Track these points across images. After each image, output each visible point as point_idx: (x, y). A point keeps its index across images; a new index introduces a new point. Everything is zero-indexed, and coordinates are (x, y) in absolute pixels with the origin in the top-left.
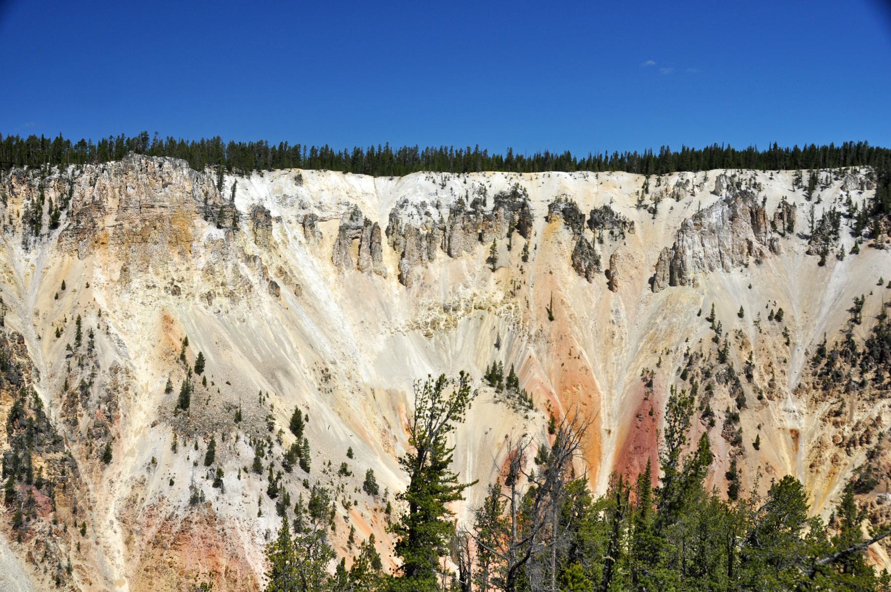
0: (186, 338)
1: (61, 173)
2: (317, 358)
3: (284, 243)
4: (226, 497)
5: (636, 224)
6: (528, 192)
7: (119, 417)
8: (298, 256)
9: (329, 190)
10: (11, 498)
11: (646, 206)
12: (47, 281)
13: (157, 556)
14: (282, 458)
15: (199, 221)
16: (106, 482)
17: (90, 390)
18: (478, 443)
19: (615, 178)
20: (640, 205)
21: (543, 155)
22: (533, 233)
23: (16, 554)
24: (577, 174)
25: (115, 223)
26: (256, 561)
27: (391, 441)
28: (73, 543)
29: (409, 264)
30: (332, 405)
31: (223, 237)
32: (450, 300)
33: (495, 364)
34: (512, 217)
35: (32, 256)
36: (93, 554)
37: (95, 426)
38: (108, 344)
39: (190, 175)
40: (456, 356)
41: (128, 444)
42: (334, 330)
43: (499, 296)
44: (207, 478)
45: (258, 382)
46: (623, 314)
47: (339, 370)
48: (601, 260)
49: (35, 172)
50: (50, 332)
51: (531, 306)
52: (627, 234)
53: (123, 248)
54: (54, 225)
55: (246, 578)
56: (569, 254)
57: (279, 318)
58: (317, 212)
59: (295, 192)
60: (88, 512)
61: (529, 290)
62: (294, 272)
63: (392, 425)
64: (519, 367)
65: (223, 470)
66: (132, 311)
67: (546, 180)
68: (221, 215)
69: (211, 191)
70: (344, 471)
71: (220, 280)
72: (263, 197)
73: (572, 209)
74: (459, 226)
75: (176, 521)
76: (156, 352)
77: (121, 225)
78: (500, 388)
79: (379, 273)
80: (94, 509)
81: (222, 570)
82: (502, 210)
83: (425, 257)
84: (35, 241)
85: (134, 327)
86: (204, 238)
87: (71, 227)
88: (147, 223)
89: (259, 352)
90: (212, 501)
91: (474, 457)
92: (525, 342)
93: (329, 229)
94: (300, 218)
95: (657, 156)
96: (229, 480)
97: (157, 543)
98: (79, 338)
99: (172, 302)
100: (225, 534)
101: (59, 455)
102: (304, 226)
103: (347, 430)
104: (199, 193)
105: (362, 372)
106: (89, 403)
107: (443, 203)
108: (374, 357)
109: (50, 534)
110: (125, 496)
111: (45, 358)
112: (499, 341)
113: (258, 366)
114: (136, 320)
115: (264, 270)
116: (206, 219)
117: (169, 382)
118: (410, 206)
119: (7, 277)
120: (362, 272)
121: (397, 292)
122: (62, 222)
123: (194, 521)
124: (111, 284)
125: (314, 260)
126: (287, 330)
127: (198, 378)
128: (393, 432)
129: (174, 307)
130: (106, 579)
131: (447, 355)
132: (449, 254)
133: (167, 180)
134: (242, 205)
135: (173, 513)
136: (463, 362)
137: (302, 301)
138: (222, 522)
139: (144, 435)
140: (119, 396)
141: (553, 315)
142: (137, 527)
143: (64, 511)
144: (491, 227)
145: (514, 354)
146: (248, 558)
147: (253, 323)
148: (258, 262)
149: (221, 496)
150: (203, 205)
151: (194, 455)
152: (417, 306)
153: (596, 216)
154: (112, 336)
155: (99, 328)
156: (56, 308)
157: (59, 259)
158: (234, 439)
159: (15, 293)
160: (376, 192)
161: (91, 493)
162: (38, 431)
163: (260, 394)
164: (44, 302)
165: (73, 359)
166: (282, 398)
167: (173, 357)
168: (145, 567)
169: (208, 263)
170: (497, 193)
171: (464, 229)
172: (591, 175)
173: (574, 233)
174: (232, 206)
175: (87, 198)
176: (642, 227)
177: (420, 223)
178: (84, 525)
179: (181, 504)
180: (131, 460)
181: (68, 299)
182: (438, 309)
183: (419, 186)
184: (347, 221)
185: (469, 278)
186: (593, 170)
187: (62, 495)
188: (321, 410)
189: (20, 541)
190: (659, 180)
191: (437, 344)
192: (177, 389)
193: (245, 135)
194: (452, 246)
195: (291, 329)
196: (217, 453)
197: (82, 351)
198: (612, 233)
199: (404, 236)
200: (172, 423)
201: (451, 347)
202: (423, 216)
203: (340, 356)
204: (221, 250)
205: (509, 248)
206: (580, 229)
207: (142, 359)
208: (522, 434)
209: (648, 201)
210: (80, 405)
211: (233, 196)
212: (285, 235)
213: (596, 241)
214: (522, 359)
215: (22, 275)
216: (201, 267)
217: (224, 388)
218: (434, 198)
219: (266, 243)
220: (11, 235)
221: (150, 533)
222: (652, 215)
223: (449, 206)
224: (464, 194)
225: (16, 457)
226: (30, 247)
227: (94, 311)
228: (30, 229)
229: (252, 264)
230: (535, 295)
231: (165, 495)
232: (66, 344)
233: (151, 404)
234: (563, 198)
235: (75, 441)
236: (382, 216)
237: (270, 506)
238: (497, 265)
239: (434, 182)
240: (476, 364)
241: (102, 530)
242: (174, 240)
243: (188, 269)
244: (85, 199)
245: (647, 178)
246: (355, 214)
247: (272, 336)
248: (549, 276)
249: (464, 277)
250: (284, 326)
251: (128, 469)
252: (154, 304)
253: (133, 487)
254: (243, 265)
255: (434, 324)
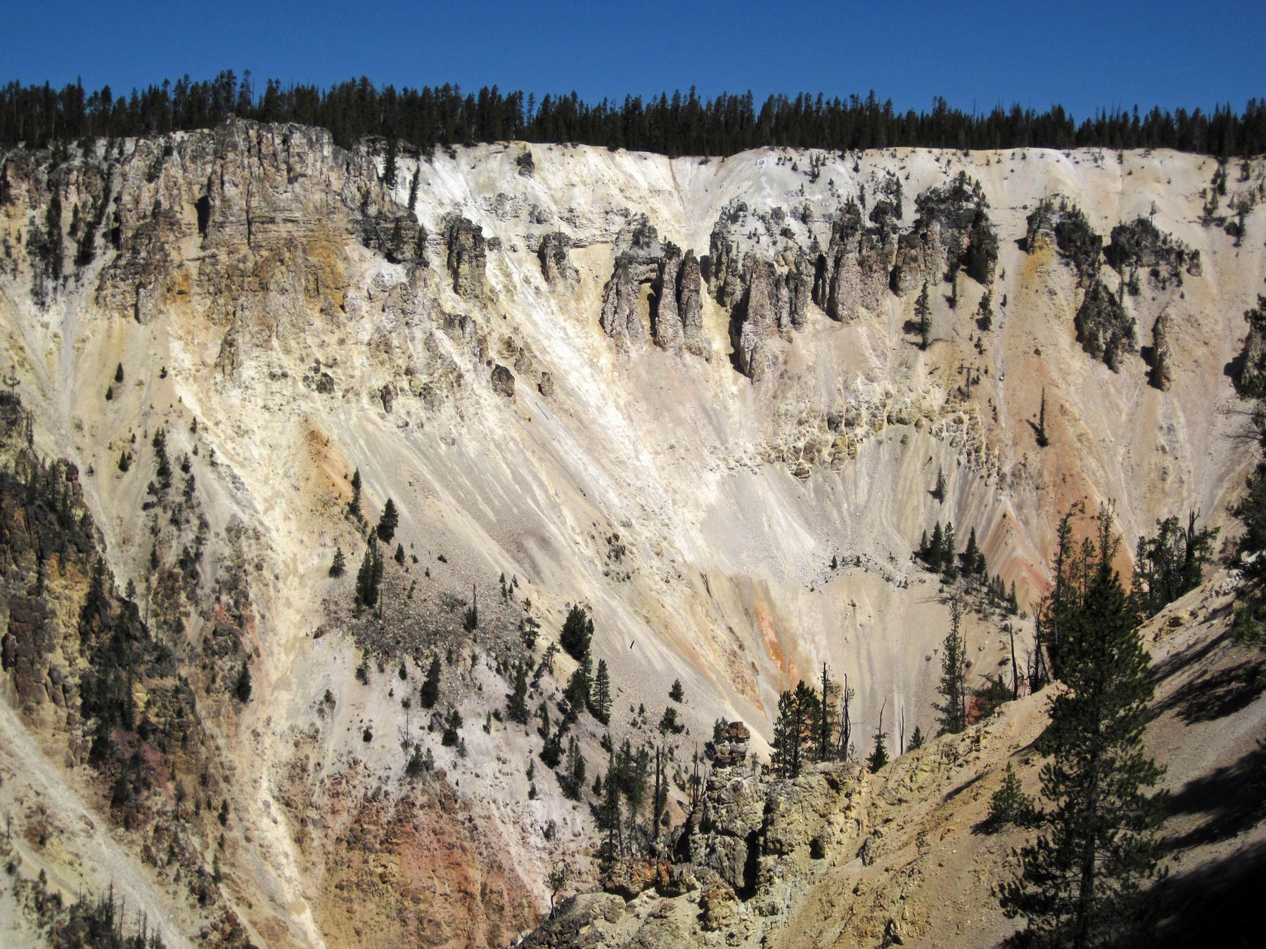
0: (357, 475)
1: (85, 155)
2: (596, 516)
3: (509, 291)
4: (469, 762)
5: (1203, 258)
6: (986, 189)
7: (253, 618)
8: (536, 317)
9: (584, 183)
10: (99, 754)
11: (1220, 221)
12: (85, 366)
13: (357, 862)
14: (560, 696)
15: (354, 248)
16: (246, 736)
17: (198, 568)
18: (913, 677)
19: (1156, 162)
20: (1209, 218)
21: (1008, 114)
22: (998, 272)
23: (125, 849)
24: (1079, 153)
25: (202, 254)
26: (533, 876)
27: (748, 673)
28: (211, 835)
29: (755, 333)
30: (632, 604)
31: (405, 280)
32: (839, 405)
33: (937, 528)
34: (956, 241)
35: (52, 318)
36: (247, 857)
37: (215, 633)
38: (216, 485)
39: (335, 158)
40: (858, 515)
41: (276, 668)
42: (621, 462)
43: (937, 398)
44: (431, 728)
45: (495, 559)
46: (1182, 434)
47: (639, 536)
48: (1137, 328)
49: (39, 154)
50: (107, 464)
51: (1002, 418)
52: (1185, 277)
53: (221, 301)
54: (85, 257)
55: (521, 905)
56: (1070, 315)
57: (518, 439)
58: (566, 229)
59: (520, 188)
60: (223, 785)
61: (995, 387)
62: (534, 348)
63: (746, 644)
64: (983, 537)
65: (462, 713)
66: (248, 423)
67: (1017, 164)
68: (397, 236)
69: (374, 188)
70: (669, 723)
71: (402, 363)
72: (459, 198)
73: (1074, 224)
74: (852, 258)
75: (385, 803)
76: (303, 501)
77: (214, 256)
78: (949, 577)
79: (697, 352)
80: (233, 781)
81: (476, 889)
82: (936, 227)
83: (785, 319)
84: (55, 289)
85: (256, 453)
86: (368, 282)
87: (123, 262)
88: (265, 253)
89: (489, 502)
90: (446, 769)
91: (908, 703)
92: (993, 488)
93: (592, 262)
94: (533, 242)
95: (1239, 117)
96: (470, 732)
97: (354, 840)
98: (164, 471)
99: (319, 405)
100: (476, 828)
101: (170, 682)
102: (542, 256)
103: (664, 649)
104: (352, 192)
105: (680, 543)
106: (199, 591)
107: (816, 212)
108: (702, 515)
109: (176, 817)
110: (284, 760)
111: (110, 504)
112: (941, 484)
113: (490, 529)
114: (257, 438)
115: (482, 342)
116: (366, 244)
117: (339, 556)
118: (750, 219)
119: (16, 358)
120: (664, 349)
121: (734, 389)
122: (99, 252)
123: (418, 803)
124: (204, 371)
125: (568, 325)
126: (533, 460)
127: (387, 550)
128: (749, 656)
129: (324, 415)
130: (272, 899)
131: (840, 512)
132: (832, 313)
133: (298, 168)
134: (428, 216)
135: (379, 789)
136: (872, 526)
137: (555, 406)
138: (466, 806)
139: (303, 652)
140: (249, 578)
141: (1046, 434)
142: (313, 814)
143: (189, 782)
144: (915, 259)
145: (973, 511)
146: (519, 870)
147: (471, 447)
148: (469, 328)
149: (460, 761)
150: (360, 218)
151: (402, 689)
152: (776, 416)
153: (1123, 239)
154: (221, 469)
155: (195, 453)
156: (111, 416)
157: (102, 324)
158: (469, 662)
159: (34, 387)
160: (677, 187)
161: (225, 752)
162: (129, 637)
163: (502, 580)
164: (89, 405)
165: (159, 510)
166: (542, 588)
167: (337, 509)
168: (336, 881)
169: (378, 330)
170: (922, 190)
171: (861, 263)
172: (1109, 155)
173: (1081, 274)
174: (414, 219)
175: (146, 204)
176: (1215, 263)
177: (772, 252)
178: (225, 807)
179: (391, 773)
180: (284, 696)
181: (129, 399)
182: (816, 423)
183: (766, 179)
184: (624, 247)
185: (875, 362)
186: (1112, 145)
187: (180, 753)
188: (614, 612)
189: (127, 826)
190: (1245, 168)
191: (818, 491)
192: (353, 567)
193: (402, 73)
194: (840, 297)
195: (541, 459)
196: (442, 686)
197: (175, 495)
198: (1155, 273)
199: (742, 278)
200: (353, 630)
201: (847, 496)
202: (779, 238)
203: (637, 512)
204: (400, 302)
205: (952, 302)
206: (1092, 265)
207: (278, 513)
208: (999, 660)
209: (1223, 210)
210: (183, 596)
211: (413, 198)
212: (508, 275)
213: (1126, 289)
214: (990, 520)
215: (41, 354)
216: (366, 338)
217: (437, 569)
218: (797, 202)
219: (478, 292)
220: (10, 277)
221: (340, 824)
222: (1233, 239)
223: (828, 217)
224: (855, 192)
225: (102, 683)
226: (48, 300)
227: (181, 422)
228: (42, 266)
229: (458, 331)
230: (1006, 394)
231: (359, 757)
232: (147, 484)
233: (308, 596)
234: (1056, 203)
235: (182, 661)
236: (692, 236)
237: (547, 780)
238: (930, 338)
239: (794, 168)
240: (899, 530)
241: (252, 816)
242: (312, 286)
243: (342, 342)
244: (142, 206)
245: (1222, 163)
246: (642, 234)
247: (508, 472)
248: (1035, 358)
249: (865, 360)
250: (529, 454)
251: (283, 712)
252: (287, 409)
253: (296, 745)
254: (439, 334)
255: (811, 450)
